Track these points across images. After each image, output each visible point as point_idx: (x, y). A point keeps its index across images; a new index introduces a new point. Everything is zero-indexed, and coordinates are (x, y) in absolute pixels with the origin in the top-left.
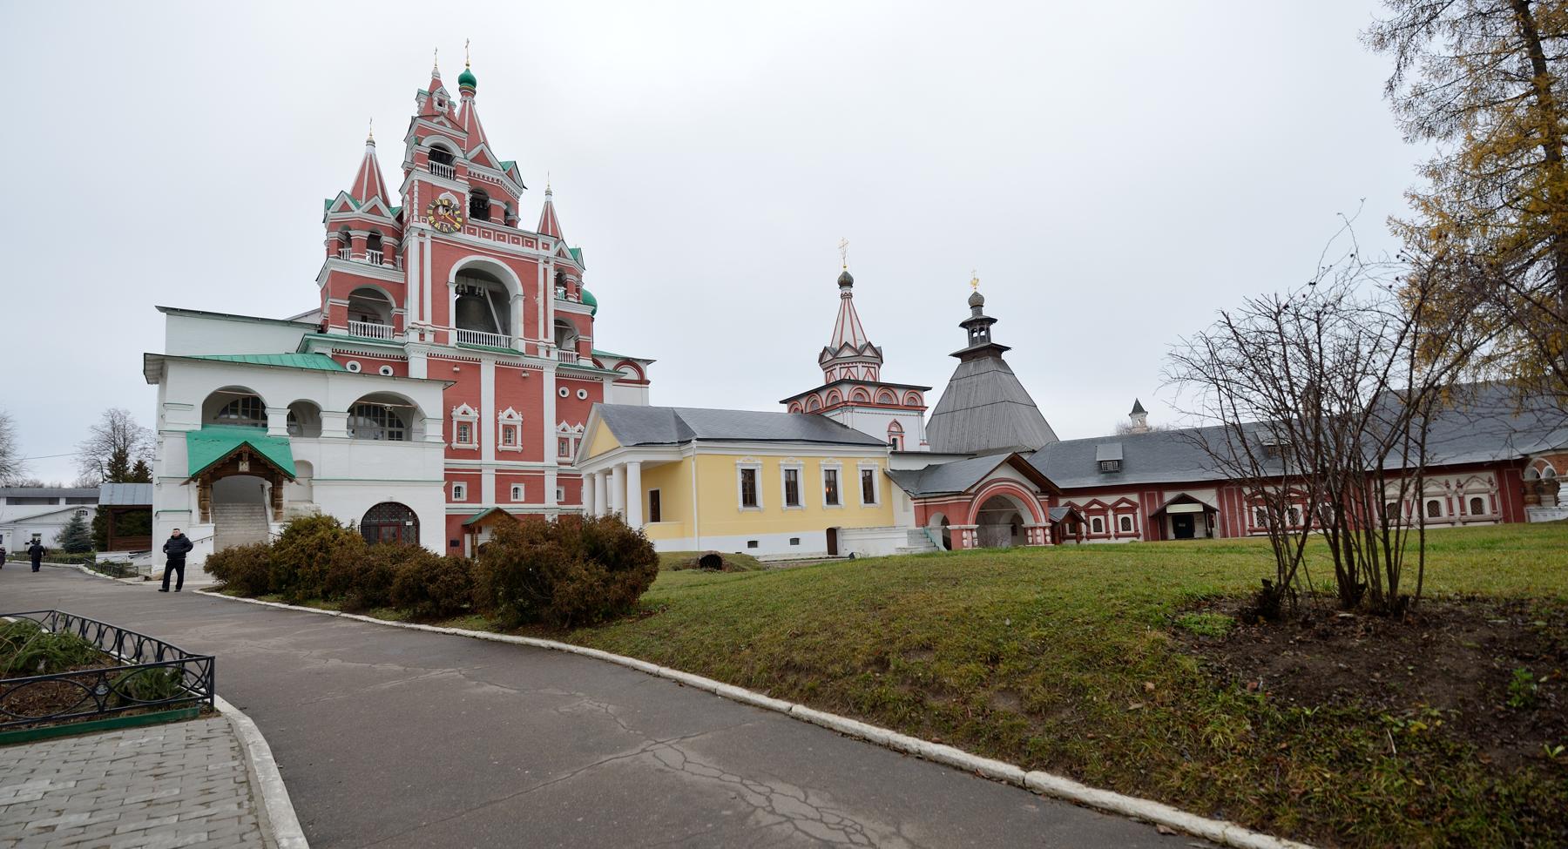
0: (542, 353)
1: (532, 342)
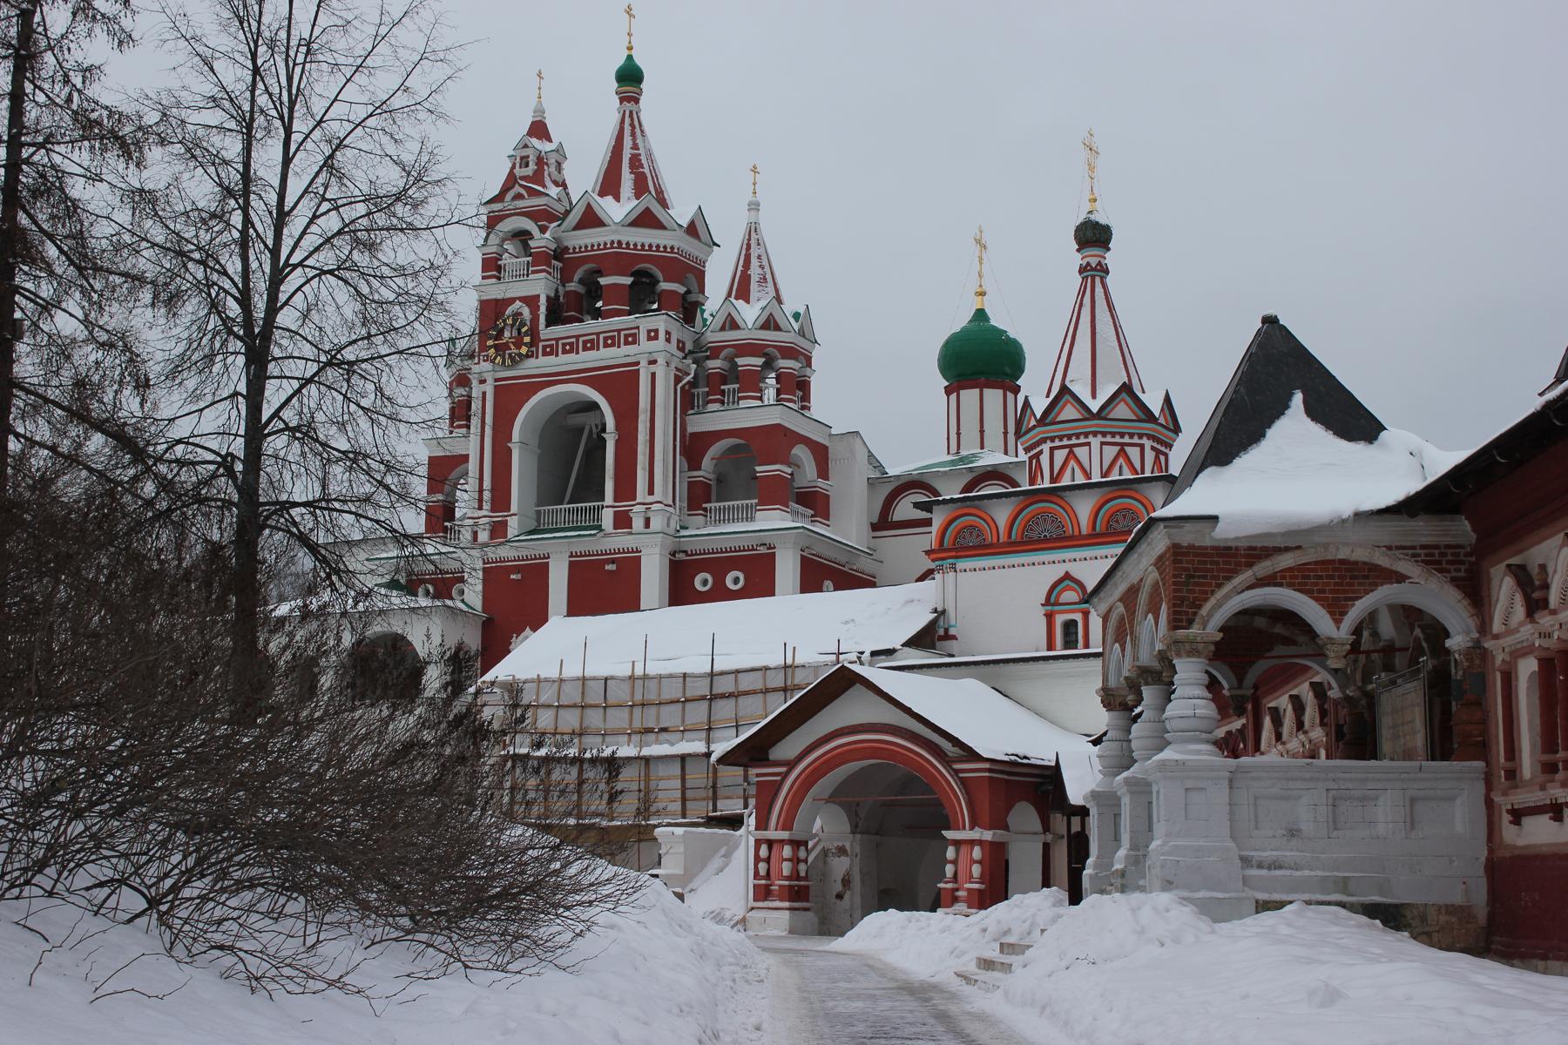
0: (638, 523)
1: (623, 506)
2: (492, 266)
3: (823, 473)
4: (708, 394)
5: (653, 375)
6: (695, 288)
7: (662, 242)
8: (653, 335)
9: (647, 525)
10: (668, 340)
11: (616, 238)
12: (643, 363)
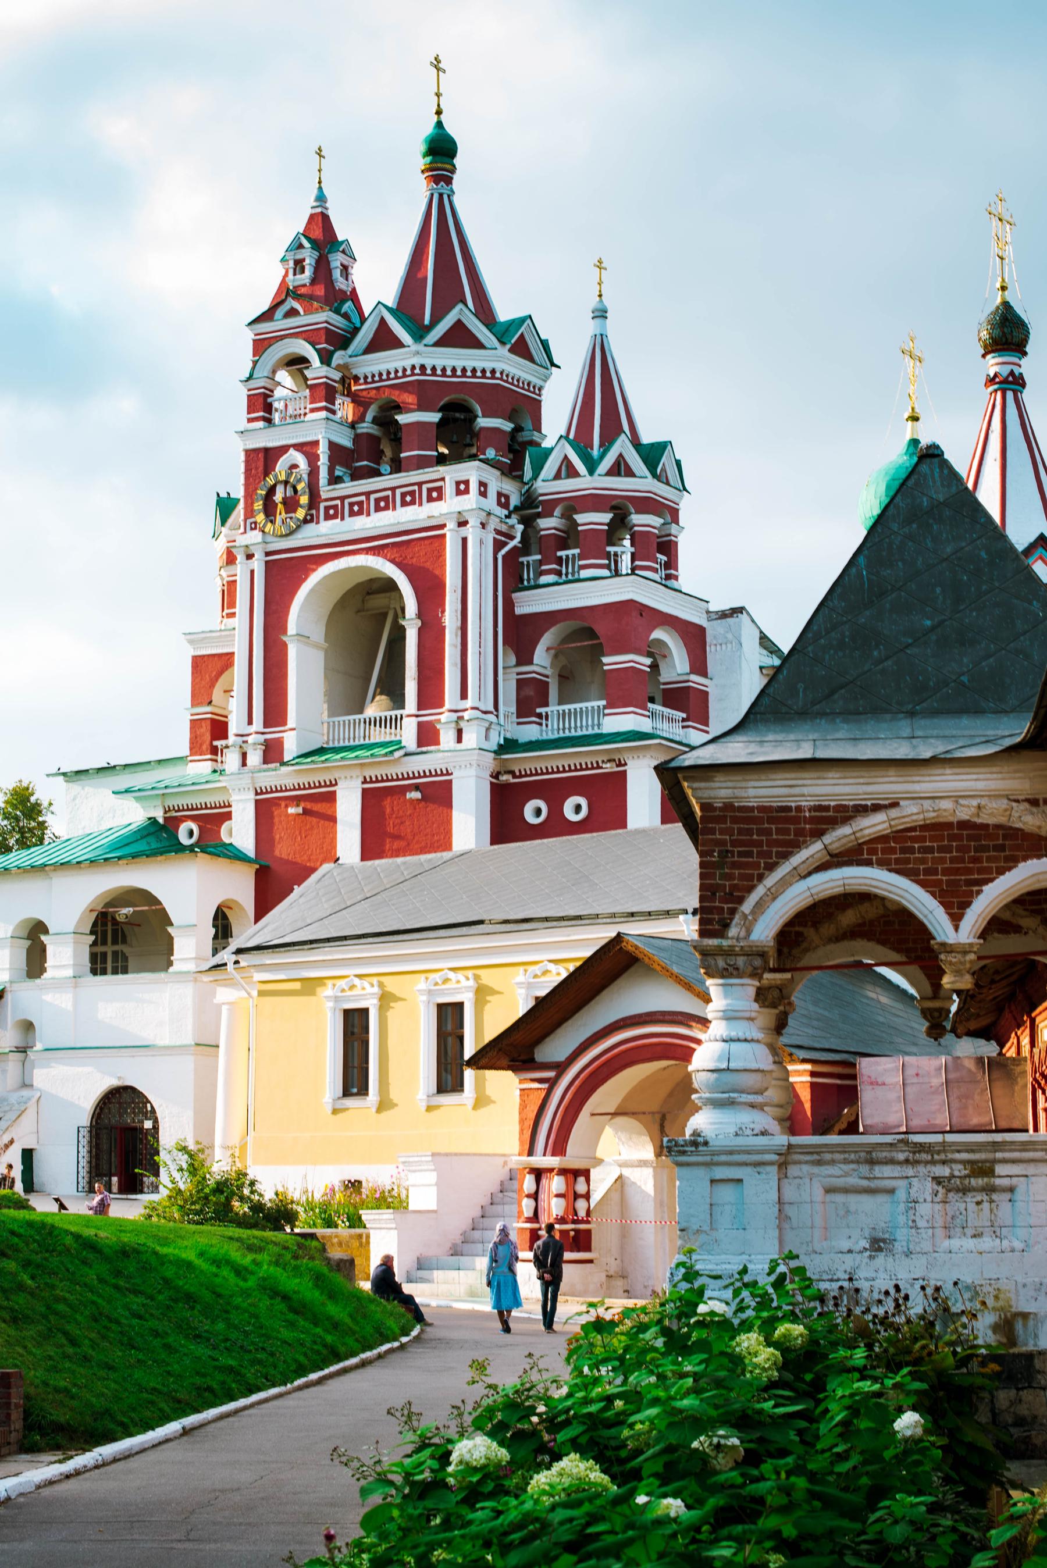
0: (447, 737)
2: (261, 405)
3: (699, 666)
4: (540, 563)
5: (464, 540)
6: (528, 424)
7: (479, 365)
8: (462, 488)
9: (459, 740)
10: (483, 494)
11: (417, 361)
12: (451, 525)
